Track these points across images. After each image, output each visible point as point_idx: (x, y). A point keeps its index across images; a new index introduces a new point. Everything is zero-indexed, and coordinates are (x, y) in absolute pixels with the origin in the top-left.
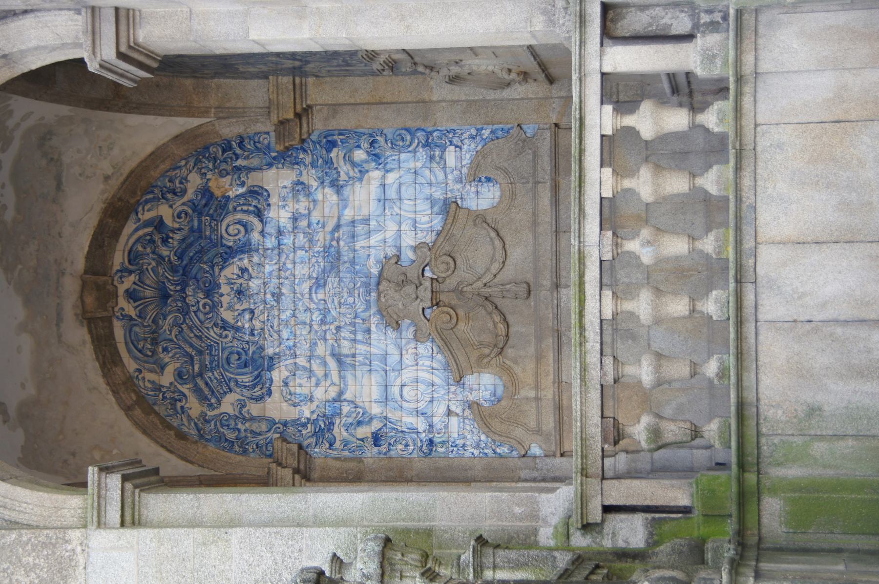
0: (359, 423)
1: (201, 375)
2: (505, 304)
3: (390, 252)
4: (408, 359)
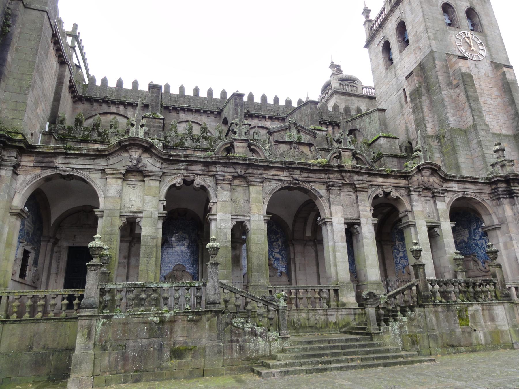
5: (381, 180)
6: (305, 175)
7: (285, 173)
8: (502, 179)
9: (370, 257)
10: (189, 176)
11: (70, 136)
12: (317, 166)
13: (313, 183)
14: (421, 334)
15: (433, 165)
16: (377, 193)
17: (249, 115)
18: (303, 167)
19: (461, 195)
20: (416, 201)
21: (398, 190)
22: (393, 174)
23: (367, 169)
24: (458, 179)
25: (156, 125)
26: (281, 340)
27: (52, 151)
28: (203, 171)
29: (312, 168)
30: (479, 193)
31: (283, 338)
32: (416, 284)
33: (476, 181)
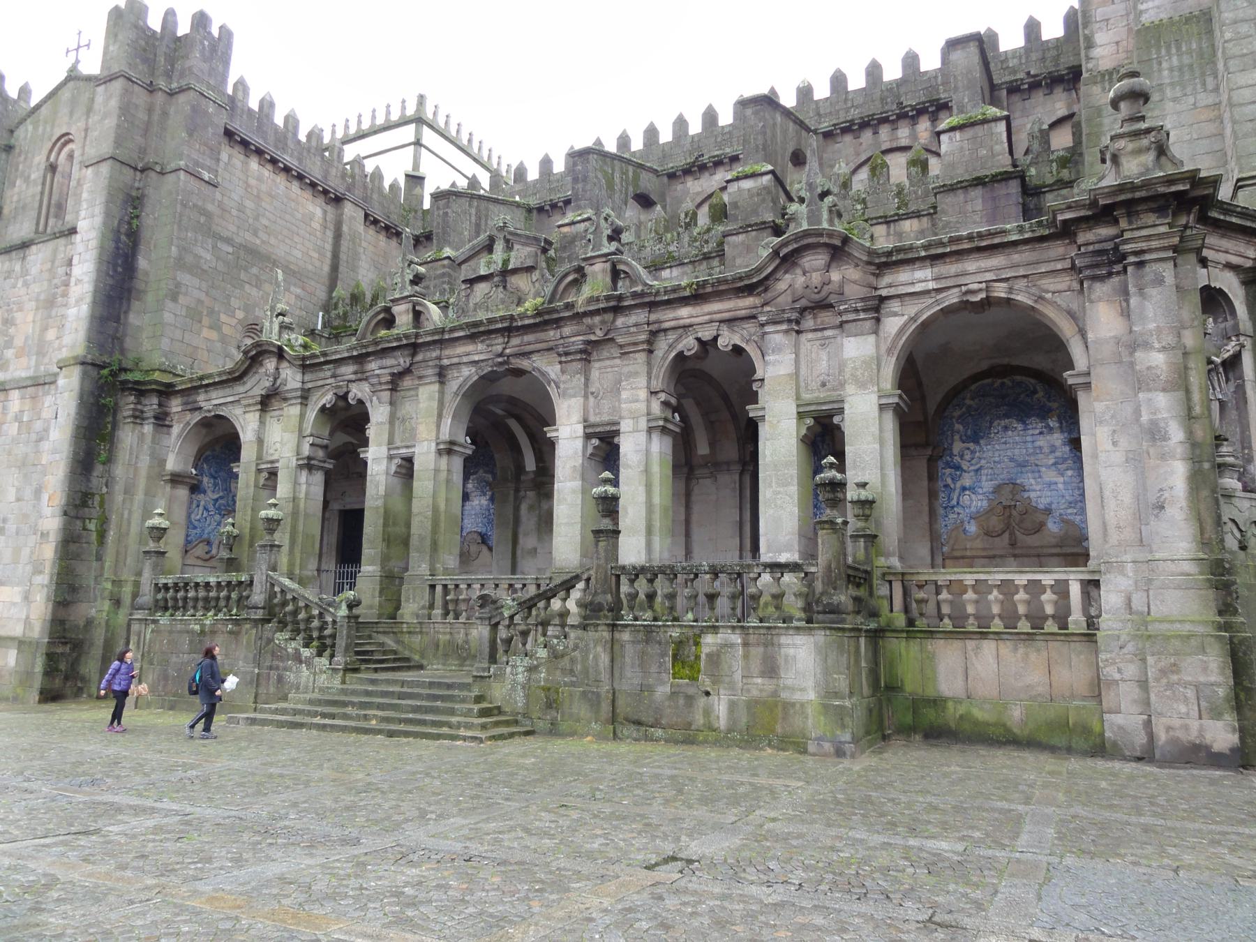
0: (953, 479)
1: (970, 415)
2: (1006, 535)
3: (1027, 488)
4: (980, 497)
5: (684, 312)
6: (515, 341)
7: (480, 347)
8: (1082, 213)
9: (631, 511)
10: (340, 387)
11: (346, 327)
12: (528, 317)
13: (536, 354)
14: (572, 688)
15: (821, 235)
16: (680, 347)
17: (698, 166)
18: (500, 326)
19: (952, 298)
20: (778, 349)
21: (735, 328)
22: (709, 289)
23: (635, 295)
24: (923, 254)
25: (439, 272)
26: (330, 672)
27: (189, 386)
28: (355, 373)
29: (520, 324)
30: (1024, 276)
31: (333, 669)
32: (585, 576)
33: (996, 241)
